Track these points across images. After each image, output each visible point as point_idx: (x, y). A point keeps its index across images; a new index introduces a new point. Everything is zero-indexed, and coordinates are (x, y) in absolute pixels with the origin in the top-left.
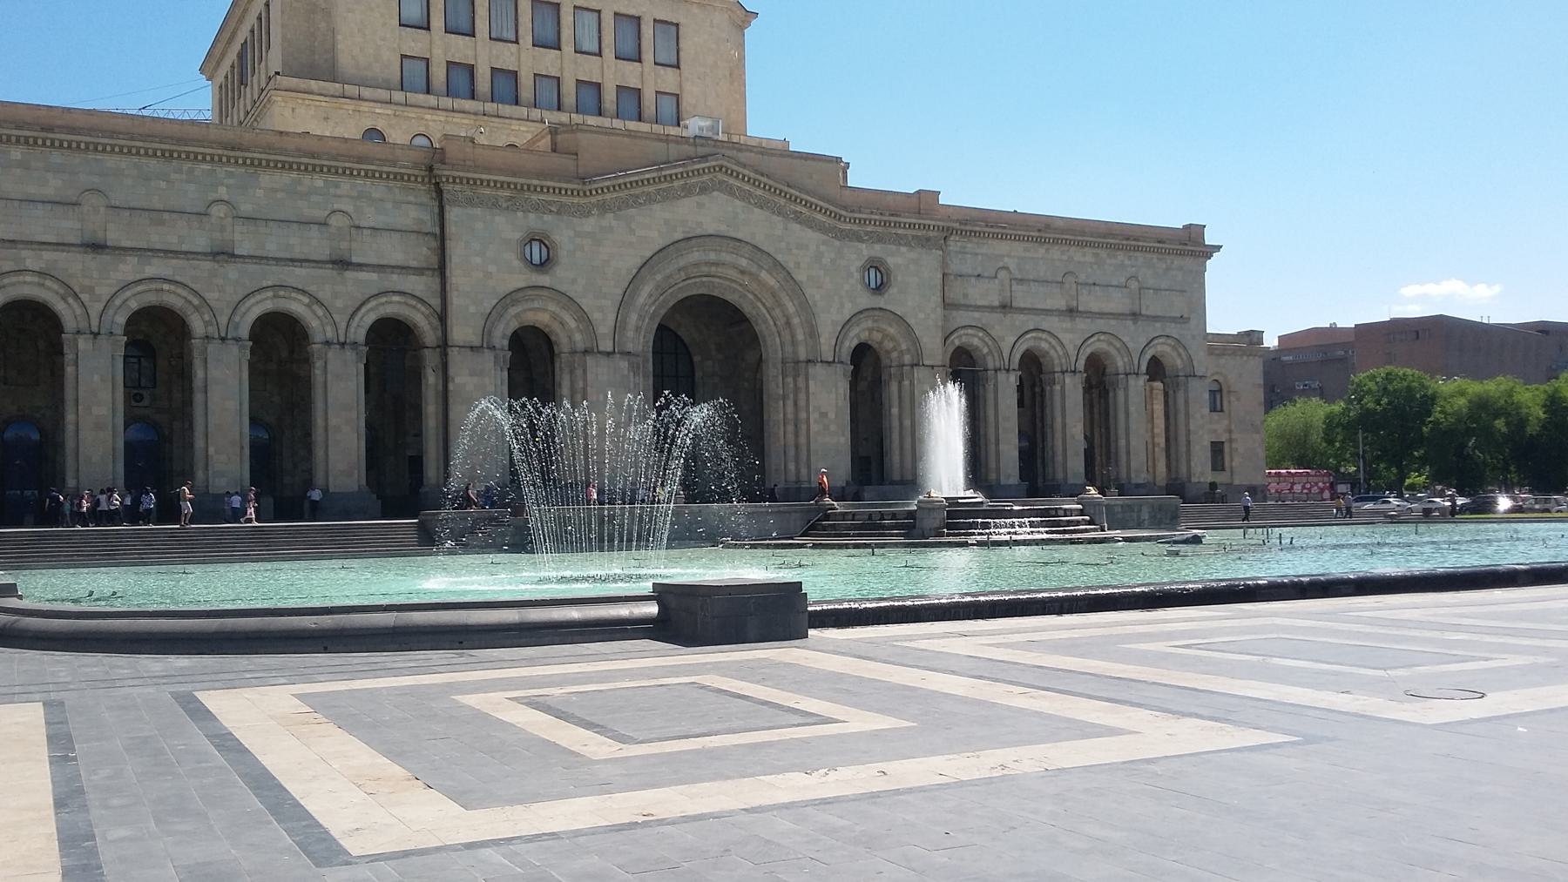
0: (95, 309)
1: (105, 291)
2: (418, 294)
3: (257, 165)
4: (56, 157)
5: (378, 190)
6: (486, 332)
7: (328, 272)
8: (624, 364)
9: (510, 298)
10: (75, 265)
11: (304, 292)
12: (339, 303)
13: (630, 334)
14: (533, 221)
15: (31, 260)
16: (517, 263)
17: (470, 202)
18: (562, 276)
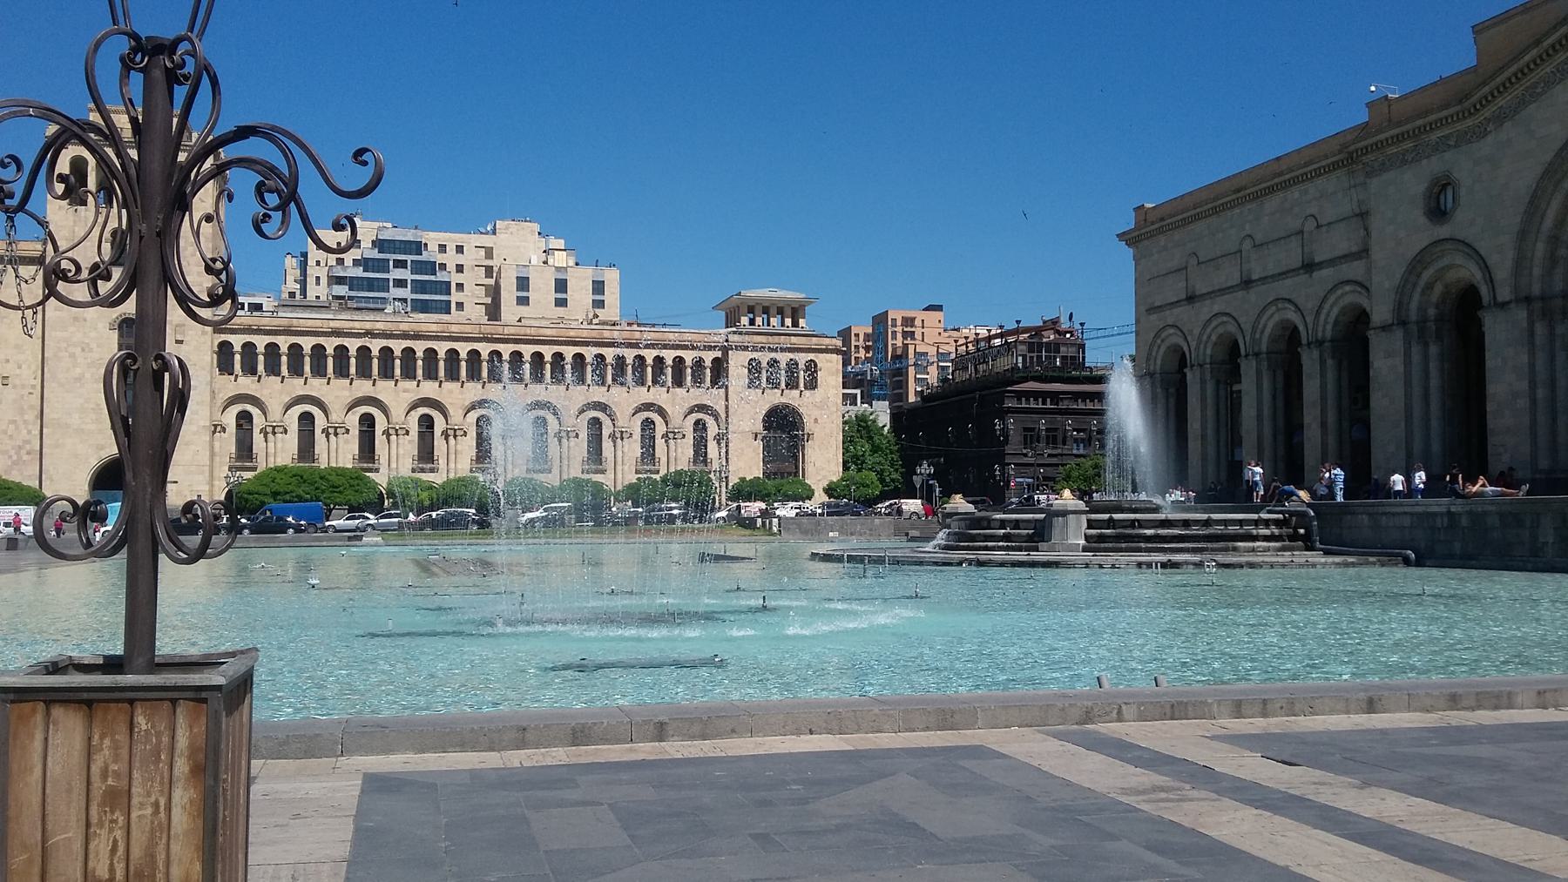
0: (1193, 345)
1: (1196, 332)
2: (1359, 279)
3: (1256, 197)
4: (1177, 235)
5: (1329, 183)
6: (1400, 306)
7: (1304, 277)
8: (1521, 314)
9: (1419, 262)
10: (1182, 314)
11: (1289, 301)
12: (1310, 305)
13: (1537, 271)
14: (1433, 166)
15: (1170, 316)
16: (1423, 220)
17: (1384, 168)
18: (1465, 223)
